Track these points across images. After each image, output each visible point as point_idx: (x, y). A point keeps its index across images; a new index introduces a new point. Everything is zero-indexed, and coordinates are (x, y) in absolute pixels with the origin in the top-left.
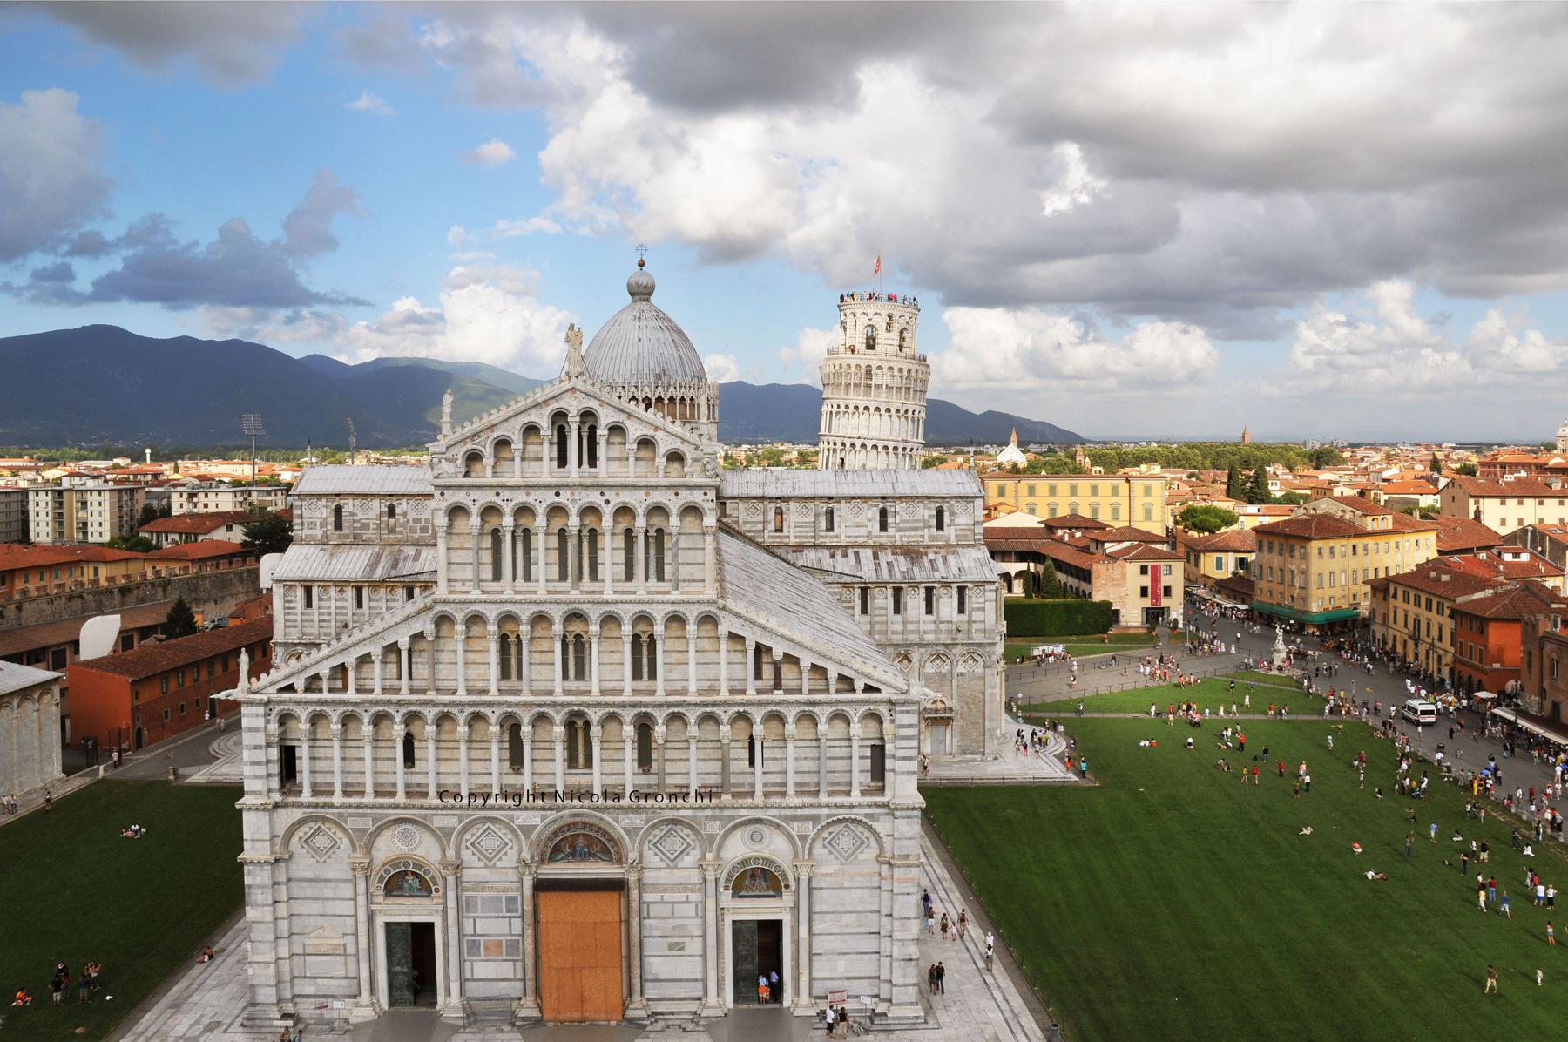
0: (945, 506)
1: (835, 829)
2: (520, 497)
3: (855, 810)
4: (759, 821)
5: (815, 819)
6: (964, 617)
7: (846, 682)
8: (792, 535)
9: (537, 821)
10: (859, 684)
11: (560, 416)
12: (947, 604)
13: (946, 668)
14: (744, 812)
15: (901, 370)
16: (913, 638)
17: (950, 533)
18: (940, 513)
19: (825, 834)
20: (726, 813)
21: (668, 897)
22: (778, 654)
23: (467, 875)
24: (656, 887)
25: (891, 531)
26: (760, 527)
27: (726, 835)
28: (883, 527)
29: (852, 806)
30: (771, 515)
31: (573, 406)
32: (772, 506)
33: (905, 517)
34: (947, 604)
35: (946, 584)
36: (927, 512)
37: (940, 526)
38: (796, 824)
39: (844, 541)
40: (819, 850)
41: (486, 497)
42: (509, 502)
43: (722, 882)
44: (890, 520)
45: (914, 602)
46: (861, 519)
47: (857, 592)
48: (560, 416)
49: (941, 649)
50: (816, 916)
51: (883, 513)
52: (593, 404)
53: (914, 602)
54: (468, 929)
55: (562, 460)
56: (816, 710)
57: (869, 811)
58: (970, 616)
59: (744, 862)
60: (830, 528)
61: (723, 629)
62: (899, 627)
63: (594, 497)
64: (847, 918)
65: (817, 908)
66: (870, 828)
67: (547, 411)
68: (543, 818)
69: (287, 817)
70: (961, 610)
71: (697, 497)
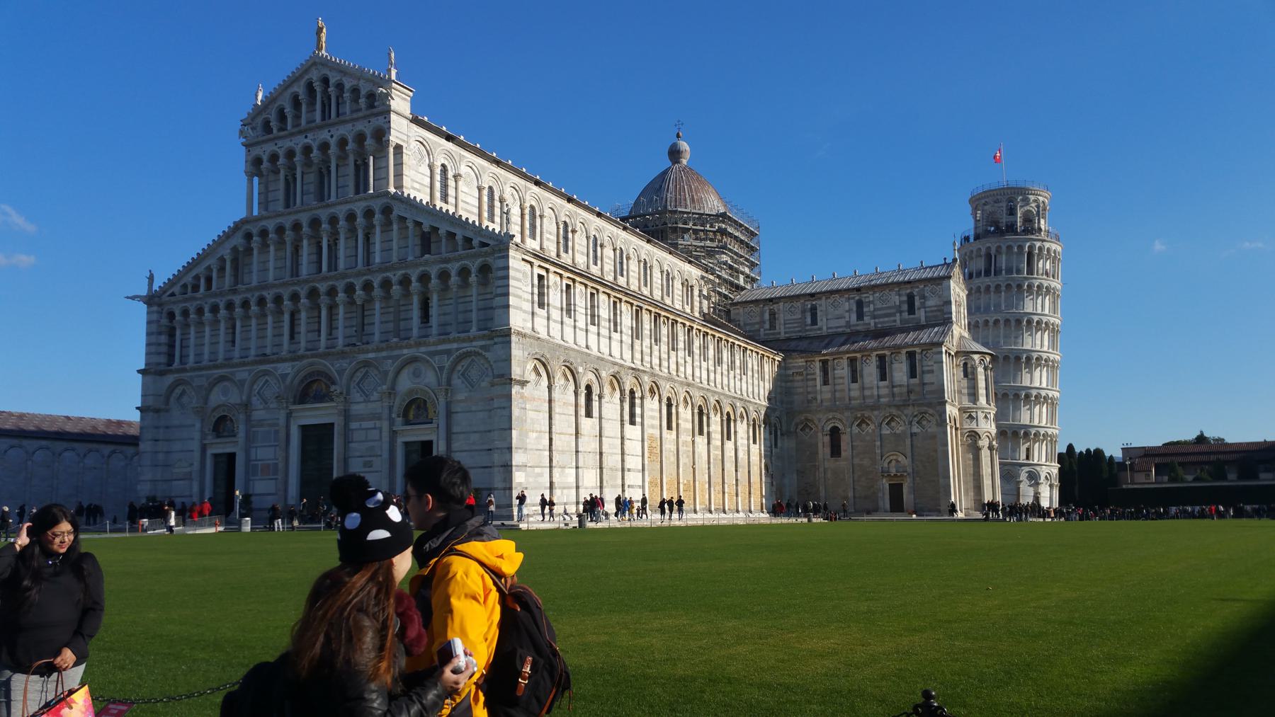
0: (916, 291)
1: (465, 363)
2: (288, 144)
3: (474, 343)
4: (414, 360)
5: (448, 352)
6: (913, 381)
9: (289, 371)
10: (475, 243)
11: (310, 86)
12: (900, 372)
13: (900, 429)
14: (405, 351)
16: (869, 401)
17: (921, 315)
18: (911, 298)
19: (459, 368)
20: (396, 353)
21: (365, 424)
23: (258, 414)
24: (361, 418)
26: (757, 326)
27: (398, 373)
28: (860, 316)
29: (471, 340)
30: (767, 316)
33: (879, 305)
35: (896, 349)
36: (895, 299)
37: (911, 310)
38: (437, 358)
39: (825, 331)
40: (457, 381)
43: (395, 409)
44: (865, 310)
45: (870, 370)
47: (818, 365)
49: (894, 411)
50: (454, 436)
51: (860, 304)
52: (326, 71)
54: (253, 457)
56: (449, 266)
57: (483, 343)
58: (921, 379)
59: (411, 392)
60: (814, 322)
61: (396, 212)
62: (855, 394)
64: (475, 437)
65: (455, 429)
67: (303, 82)
68: (293, 367)
69: (170, 379)
70: (913, 374)
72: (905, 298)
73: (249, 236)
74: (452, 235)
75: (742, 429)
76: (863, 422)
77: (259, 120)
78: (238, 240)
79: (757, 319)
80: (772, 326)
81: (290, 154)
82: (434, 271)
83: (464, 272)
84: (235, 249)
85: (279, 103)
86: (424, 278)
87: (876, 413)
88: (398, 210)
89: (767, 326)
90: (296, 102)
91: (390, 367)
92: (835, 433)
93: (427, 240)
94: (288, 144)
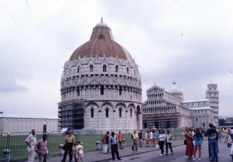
2: (152, 93)
7: (173, 104)
12: (204, 112)
16: (200, 115)
17: (205, 105)
18: (204, 103)
28: (199, 105)
30: (187, 105)
31: (155, 87)
34: (204, 112)
35: (204, 110)
36: (203, 103)
37: (204, 104)
42: (151, 94)
45: (201, 112)
46: (196, 104)
47: (195, 111)
48: (154, 88)
51: (199, 104)
53: (201, 112)
60: (193, 105)
63: (156, 93)
70: (205, 112)
71: (163, 92)
73: (147, 102)
74: (171, 104)
75: (188, 119)
76: (200, 117)
78: (146, 102)
80: (188, 106)
82: (169, 107)
83: (173, 107)
84: (146, 104)
86: (168, 107)
88: (165, 101)
90: (152, 89)
92: (197, 119)
93: (168, 104)
94: (152, 93)
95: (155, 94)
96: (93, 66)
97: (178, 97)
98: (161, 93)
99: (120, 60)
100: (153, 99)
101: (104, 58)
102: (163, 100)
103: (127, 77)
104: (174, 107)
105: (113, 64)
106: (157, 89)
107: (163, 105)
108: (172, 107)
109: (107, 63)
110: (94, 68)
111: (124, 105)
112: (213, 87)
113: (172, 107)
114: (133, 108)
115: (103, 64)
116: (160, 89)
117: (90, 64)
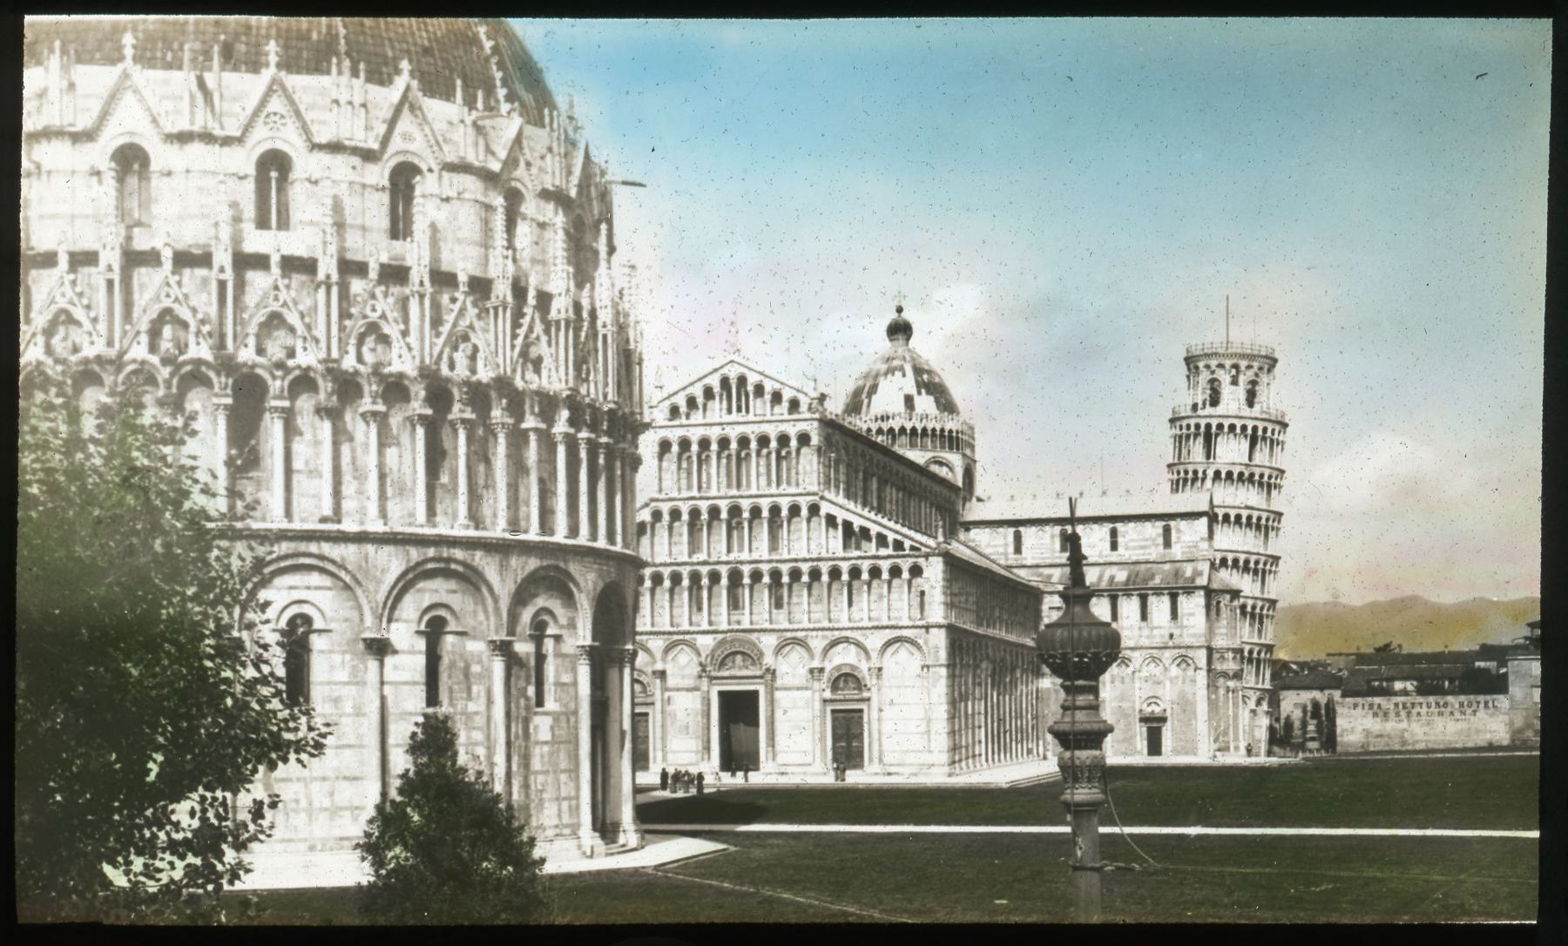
7: (898, 545)
8: (1029, 556)
10: (907, 543)
15: (1244, 428)
22: (856, 528)
25: (1121, 550)
28: (1114, 546)
30: (1011, 538)
31: (733, 373)
32: (1012, 530)
33: (1135, 536)
37: (1167, 543)
41: (680, 432)
42: (695, 435)
44: (1120, 539)
48: (725, 382)
51: (1114, 533)
52: (745, 371)
55: (729, 411)
61: (823, 512)
66: (919, 648)
72: (1161, 531)
77: (667, 403)
79: (1002, 541)
80: (1018, 550)
81: (704, 444)
85: (689, 391)
87: (1136, 654)
88: (825, 508)
89: (1011, 549)
90: (709, 394)
91: (817, 643)
93: (853, 536)
95: (733, 433)
96: (154, 166)
97: (935, 468)
98: (793, 431)
99: (443, 112)
100: (717, 488)
101: (267, 74)
102: (804, 503)
103: (502, 290)
104: (905, 565)
105: (368, 156)
106: (750, 388)
107: (810, 543)
108: (885, 565)
109: (305, 129)
110: (156, 182)
111: (471, 579)
112: (1235, 382)
113: (885, 565)
114: (556, 605)
115: (262, 139)
116: (777, 398)
117: (110, 140)
